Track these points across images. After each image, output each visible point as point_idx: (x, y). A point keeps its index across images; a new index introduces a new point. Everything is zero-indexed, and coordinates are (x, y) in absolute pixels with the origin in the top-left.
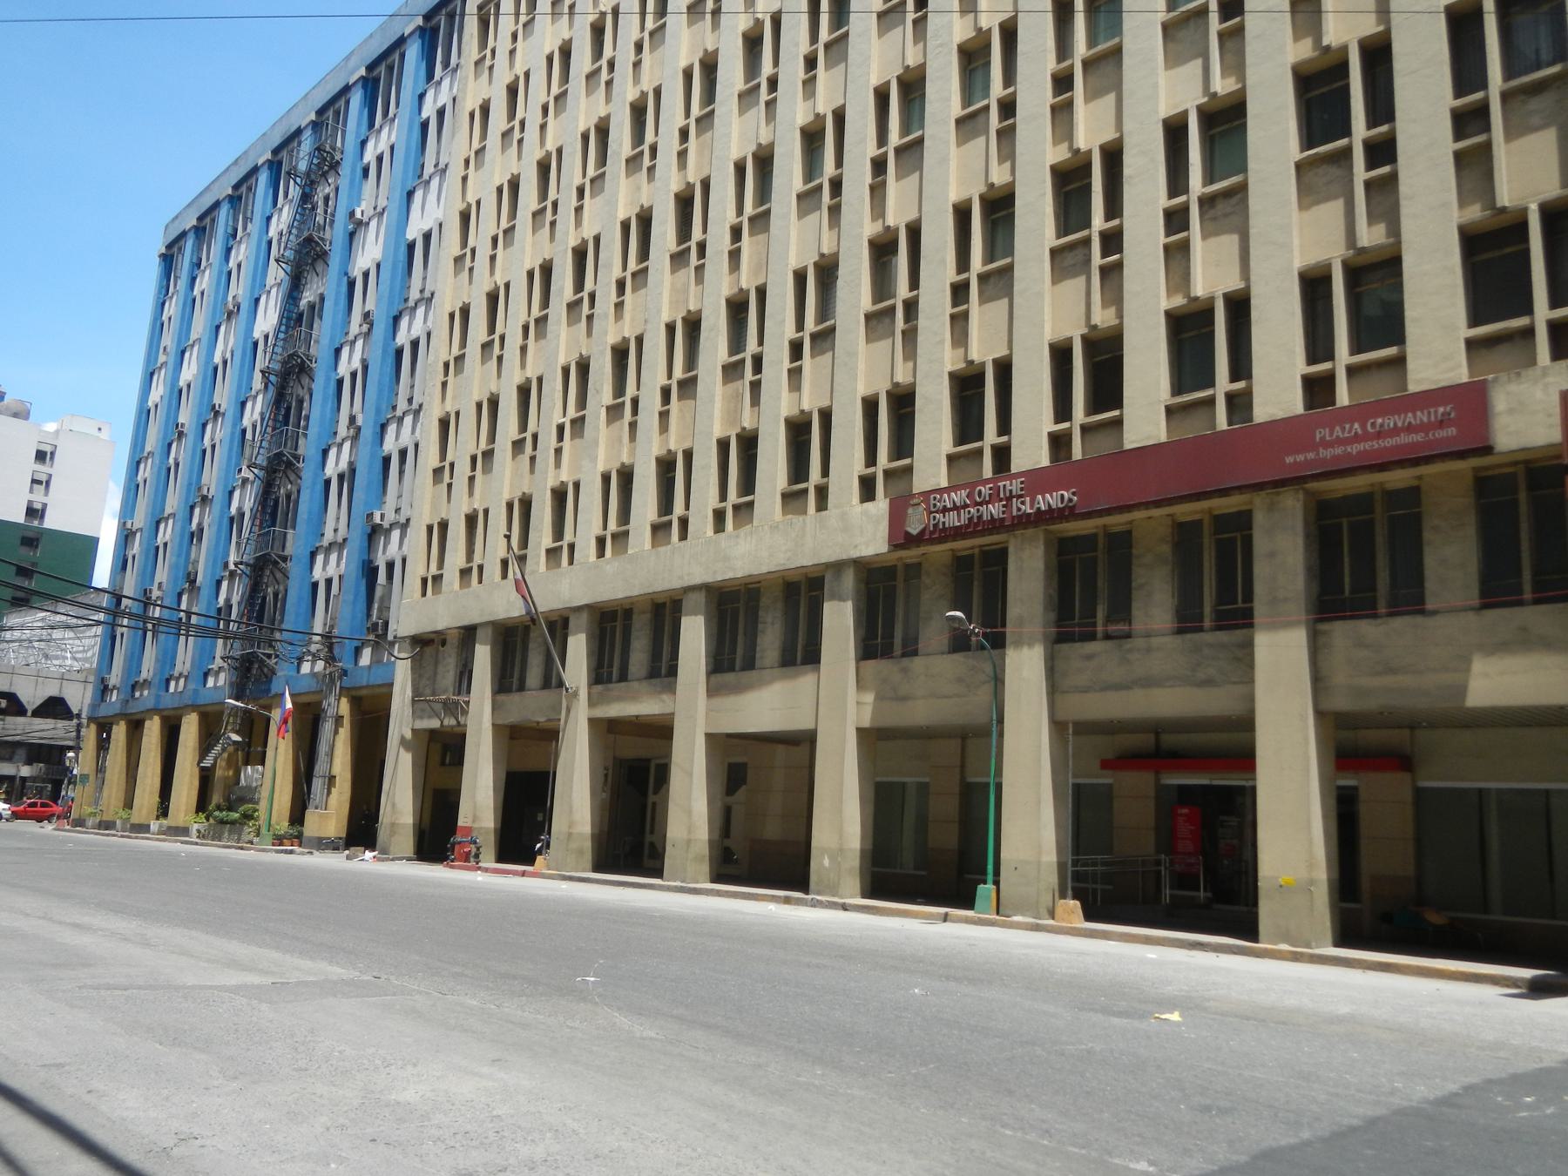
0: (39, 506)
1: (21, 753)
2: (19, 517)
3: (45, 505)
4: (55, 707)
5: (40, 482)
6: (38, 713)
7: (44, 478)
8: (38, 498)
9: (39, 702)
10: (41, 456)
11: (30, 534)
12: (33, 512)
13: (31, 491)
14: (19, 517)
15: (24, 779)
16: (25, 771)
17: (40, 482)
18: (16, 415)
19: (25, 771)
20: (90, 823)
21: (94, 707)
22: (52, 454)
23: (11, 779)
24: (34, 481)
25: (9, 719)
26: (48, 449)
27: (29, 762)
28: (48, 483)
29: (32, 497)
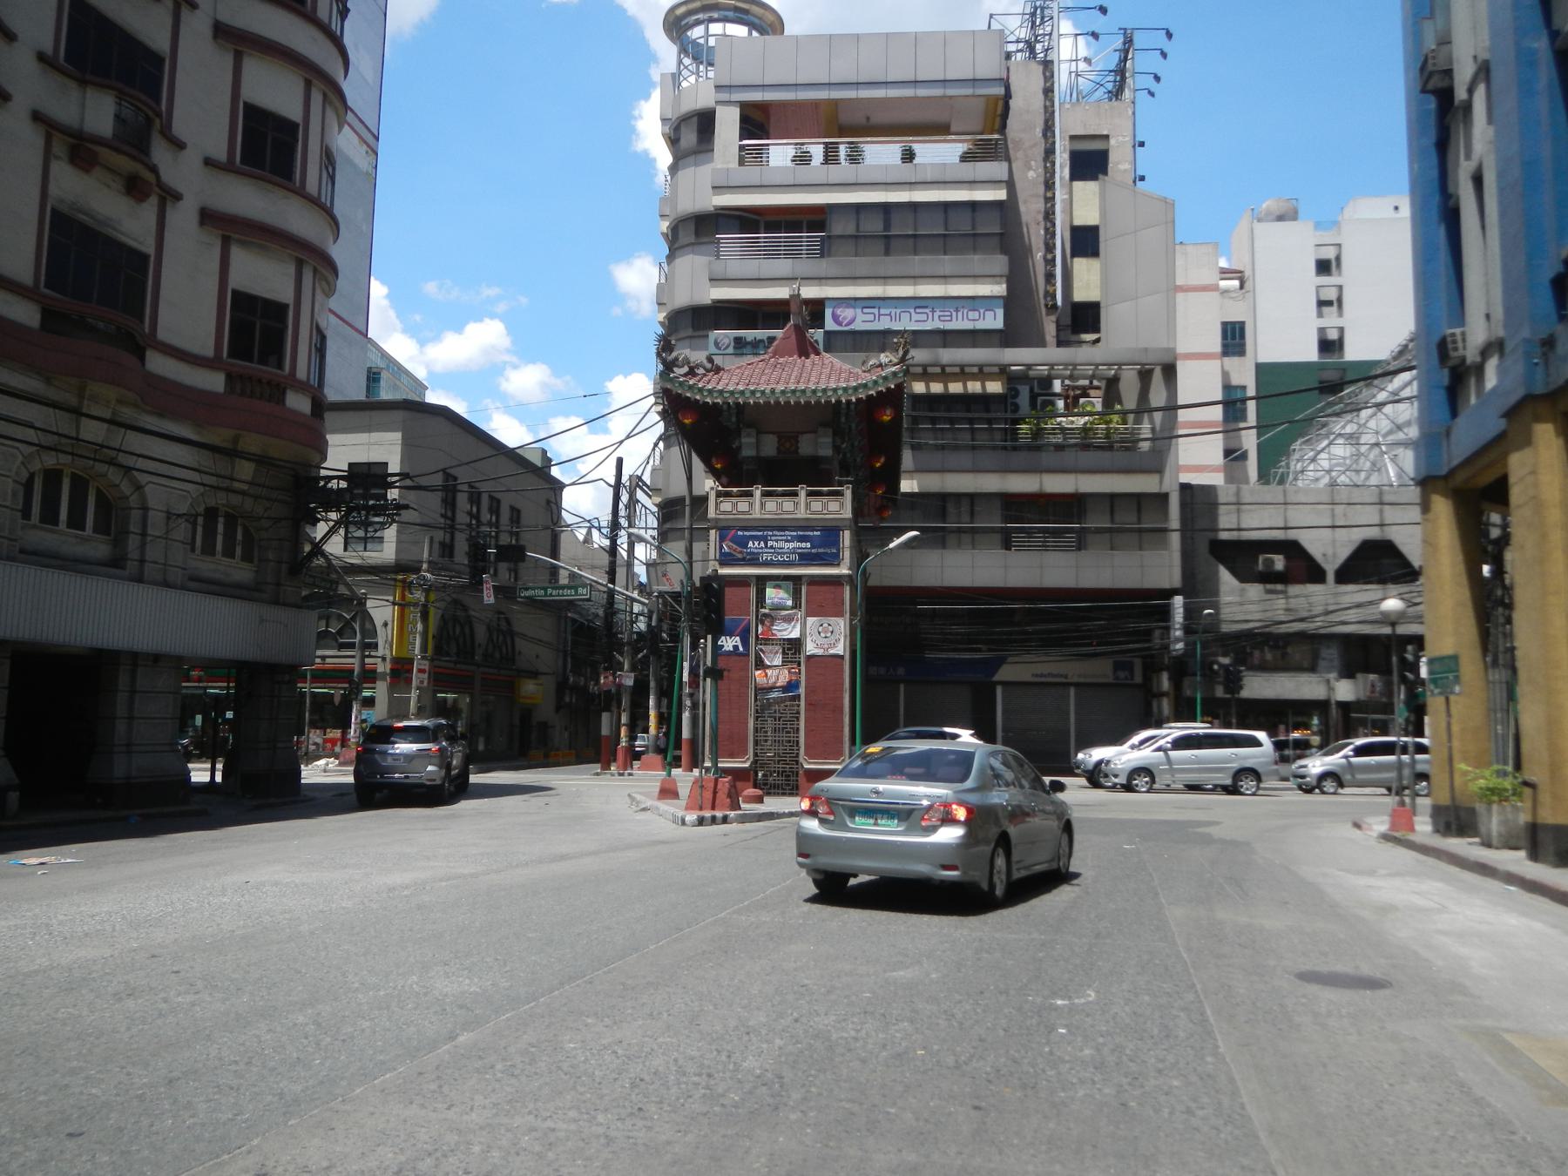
0: (1333, 335)
1: (1331, 653)
2: (1310, 354)
3: (1341, 330)
4: (1377, 562)
5: (1329, 303)
6: (1352, 571)
7: (1331, 294)
8: (1331, 320)
9: (1344, 553)
10: (1323, 267)
11: (1331, 376)
12: (1329, 346)
13: (1320, 315)
14: (1310, 354)
15: (1344, 706)
16: (1345, 691)
17: (1329, 303)
18: (1280, 218)
19: (1345, 691)
20: (1494, 822)
21: (1431, 441)
22: (1338, 259)
23: (1321, 706)
24: (1322, 304)
25: (1294, 589)
26: (1329, 254)
27: (1348, 673)
28: (1340, 300)
29: (1323, 323)
